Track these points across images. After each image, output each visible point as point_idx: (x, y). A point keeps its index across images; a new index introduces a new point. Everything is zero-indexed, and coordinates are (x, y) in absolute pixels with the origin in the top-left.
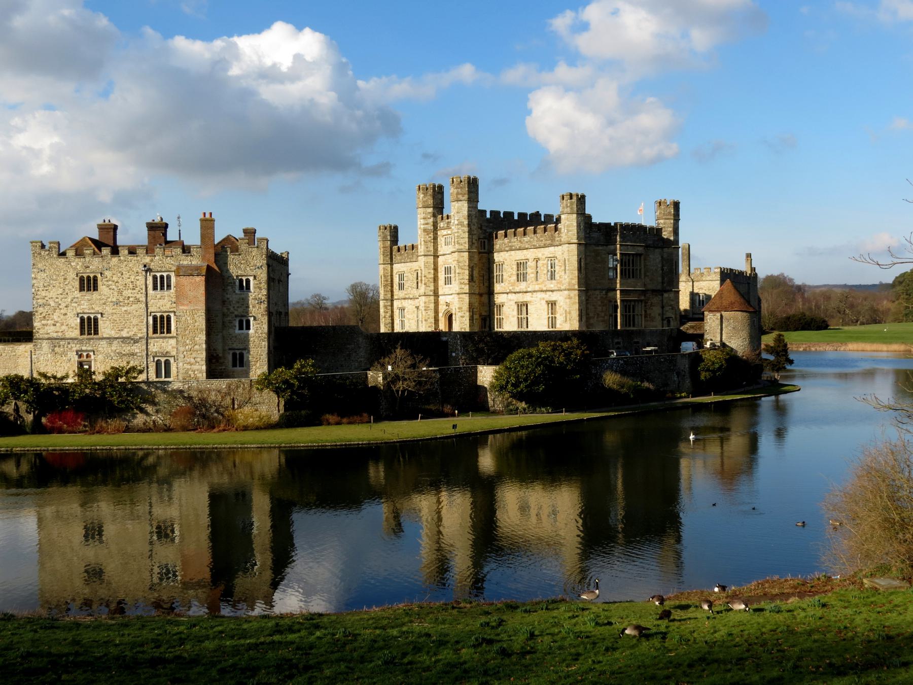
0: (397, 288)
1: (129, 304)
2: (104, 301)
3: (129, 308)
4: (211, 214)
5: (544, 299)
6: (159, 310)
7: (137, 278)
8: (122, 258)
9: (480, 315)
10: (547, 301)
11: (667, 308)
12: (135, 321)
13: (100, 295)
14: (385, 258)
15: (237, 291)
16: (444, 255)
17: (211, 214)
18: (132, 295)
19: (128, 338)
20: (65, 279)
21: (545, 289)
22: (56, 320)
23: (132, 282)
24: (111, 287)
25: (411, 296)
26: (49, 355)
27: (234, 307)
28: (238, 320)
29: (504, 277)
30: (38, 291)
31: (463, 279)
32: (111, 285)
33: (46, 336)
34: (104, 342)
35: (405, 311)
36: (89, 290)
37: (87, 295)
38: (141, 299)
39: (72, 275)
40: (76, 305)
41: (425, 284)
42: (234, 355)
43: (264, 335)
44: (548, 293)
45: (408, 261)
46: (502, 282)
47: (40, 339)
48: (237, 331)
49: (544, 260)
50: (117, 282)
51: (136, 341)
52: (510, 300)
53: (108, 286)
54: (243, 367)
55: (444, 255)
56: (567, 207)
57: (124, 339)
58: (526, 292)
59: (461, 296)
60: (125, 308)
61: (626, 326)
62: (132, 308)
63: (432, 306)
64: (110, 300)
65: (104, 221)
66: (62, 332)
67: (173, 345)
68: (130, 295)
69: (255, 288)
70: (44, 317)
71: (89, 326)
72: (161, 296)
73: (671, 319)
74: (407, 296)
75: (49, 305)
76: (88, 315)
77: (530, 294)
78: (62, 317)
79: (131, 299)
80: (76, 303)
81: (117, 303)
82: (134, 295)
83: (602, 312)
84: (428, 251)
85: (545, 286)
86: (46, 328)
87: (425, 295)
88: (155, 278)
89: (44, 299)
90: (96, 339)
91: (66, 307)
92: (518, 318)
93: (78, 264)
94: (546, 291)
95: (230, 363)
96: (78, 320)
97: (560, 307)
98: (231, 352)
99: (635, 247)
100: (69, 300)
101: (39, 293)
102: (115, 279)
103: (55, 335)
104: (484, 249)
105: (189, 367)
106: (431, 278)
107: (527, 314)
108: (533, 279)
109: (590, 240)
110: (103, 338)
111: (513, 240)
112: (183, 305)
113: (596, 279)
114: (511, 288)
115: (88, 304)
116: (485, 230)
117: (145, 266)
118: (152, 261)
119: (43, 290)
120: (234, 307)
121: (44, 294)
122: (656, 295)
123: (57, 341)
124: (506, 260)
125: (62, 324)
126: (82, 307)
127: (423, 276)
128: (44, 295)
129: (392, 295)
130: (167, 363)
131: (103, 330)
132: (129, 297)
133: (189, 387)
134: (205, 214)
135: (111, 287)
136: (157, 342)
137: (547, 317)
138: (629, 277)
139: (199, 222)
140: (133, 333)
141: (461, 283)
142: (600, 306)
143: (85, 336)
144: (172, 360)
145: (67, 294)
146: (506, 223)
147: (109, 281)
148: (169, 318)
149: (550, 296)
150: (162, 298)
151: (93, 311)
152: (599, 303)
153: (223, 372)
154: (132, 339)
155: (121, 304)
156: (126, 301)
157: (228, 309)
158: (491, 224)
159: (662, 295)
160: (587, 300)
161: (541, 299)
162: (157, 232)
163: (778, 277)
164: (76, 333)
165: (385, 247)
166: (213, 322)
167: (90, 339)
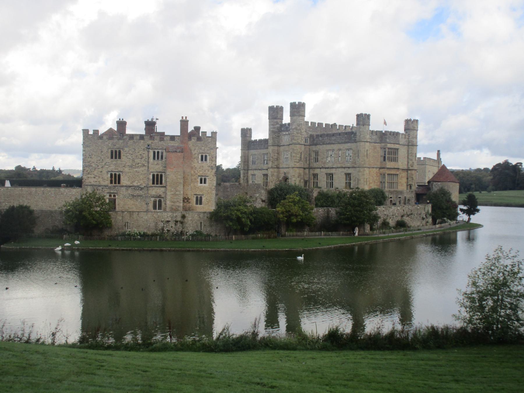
0: (251, 163)
1: (138, 167)
2: (124, 165)
3: (139, 169)
4: (186, 117)
5: (343, 172)
6: (155, 171)
7: (144, 152)
9: (304, 180)
10: (345, 173)
11: (410, 179)
12: (141, 177)
15: (200, 162)
16: (284, 145)
17: (186, 117)
19: (138, 186)
21: (344, 166)
22: (96, 175)
23: (141, 155)
24: (128, 157)
25: (260, 168)
27: (197, 171)
28: (199, 178)
29: (319, 159)
30: (86, 158)
31: (296, 159)
32: (128, 156)
33: (90, 184)
34: (124, 189)
35: (256, 176)
36: (116, 158)
37: (114, 161)
38: (145, 165)
39: (105, 150)
40: (108, 166)
41: (272, 162)
42: (197, 198)
43: (214, 187)
44: (346, 169)
45: (258, 148)
46: (318, 162)
47: (87, 185)
48: (199, 185)
49: (344, 150)
50: (132, 154)
51: (142, 189)
52: (322, 172)
53: (126, 156)
54: (201, 204)
55: (284, 145)
57: (136, 188)
58: (333, 168)
59: (294, 169)
60: (136, 169)
61: (389, 188)
62: (140, 169)
63: (275, 174)
64: (128, 164)
65: (120, 119)
66: (99, 182)
67: (163, 191)
68: (139, 162)
69: (210, 160)
70: (89, 173)
73: (412, 185)
74: (257, 168)
75: (92, 166)
76: (115, 173)
77: (335, 169)
78: (100, 173)
79: (140, 164)
81: (131, 167)
82: (142, 162)
83: (376, 180)
84: (274, 143)
85: (344, 165)
86: (90, 179)
87: (272, 168)
88: (154, 153)
89: (89, 162)
90: (119, 186)
92: (327, 182)
93: (110, 143)
94: (344, 168)
95: (195, 203)
96: (109, 175)
97: (353, 177)
98: (195, 196)
99: (395, 145)
100: (104, 164)
102: (131, 152)
103: (95, 183)
104: (307, 143)
105: (173, 204)
106: (275, 158)
107: (332, 180)
108: (337, 161)
109: (372, 140)
110: (122, 186)
111: (325, 139)
112: (171, 169)
113: (374, 162)
114: (323, 165)
116: (308, 133)
117: (149, 146)
118: (152, 143)
119: (89, 158)
120: (197, 171)
122: (404, 172)
123: (96, 187)
124: (320, 150)
125: (99, 177)
126: (111, 168)
127: (271, 157)
129: (248, 167)
130: (160, 201)
132: (138, 163)
134: (183, 117)
136: (154, 189)
137: (345, 182)
138: (392, 161)
140: (140, 183)
141: (295, 162)
142: (375, 177)
144: (162, 200)
145: (103, 160)
146: (319, 129)
147: (127, 153)
148: (161, 176)
149: (347, 170)
150: (157, 164)
151: (117, 171)
152: (375, 175)
153: (190, 208)
154: (140, 187)
155: (134, 167)
156: (137, 165)
157: (194, 172)
158: (311, 130)
159: (407, 172)
160: (369, 173)
161: (341, 172)
164: (108, 182)
166: (186, 179)
167: (115, 186)
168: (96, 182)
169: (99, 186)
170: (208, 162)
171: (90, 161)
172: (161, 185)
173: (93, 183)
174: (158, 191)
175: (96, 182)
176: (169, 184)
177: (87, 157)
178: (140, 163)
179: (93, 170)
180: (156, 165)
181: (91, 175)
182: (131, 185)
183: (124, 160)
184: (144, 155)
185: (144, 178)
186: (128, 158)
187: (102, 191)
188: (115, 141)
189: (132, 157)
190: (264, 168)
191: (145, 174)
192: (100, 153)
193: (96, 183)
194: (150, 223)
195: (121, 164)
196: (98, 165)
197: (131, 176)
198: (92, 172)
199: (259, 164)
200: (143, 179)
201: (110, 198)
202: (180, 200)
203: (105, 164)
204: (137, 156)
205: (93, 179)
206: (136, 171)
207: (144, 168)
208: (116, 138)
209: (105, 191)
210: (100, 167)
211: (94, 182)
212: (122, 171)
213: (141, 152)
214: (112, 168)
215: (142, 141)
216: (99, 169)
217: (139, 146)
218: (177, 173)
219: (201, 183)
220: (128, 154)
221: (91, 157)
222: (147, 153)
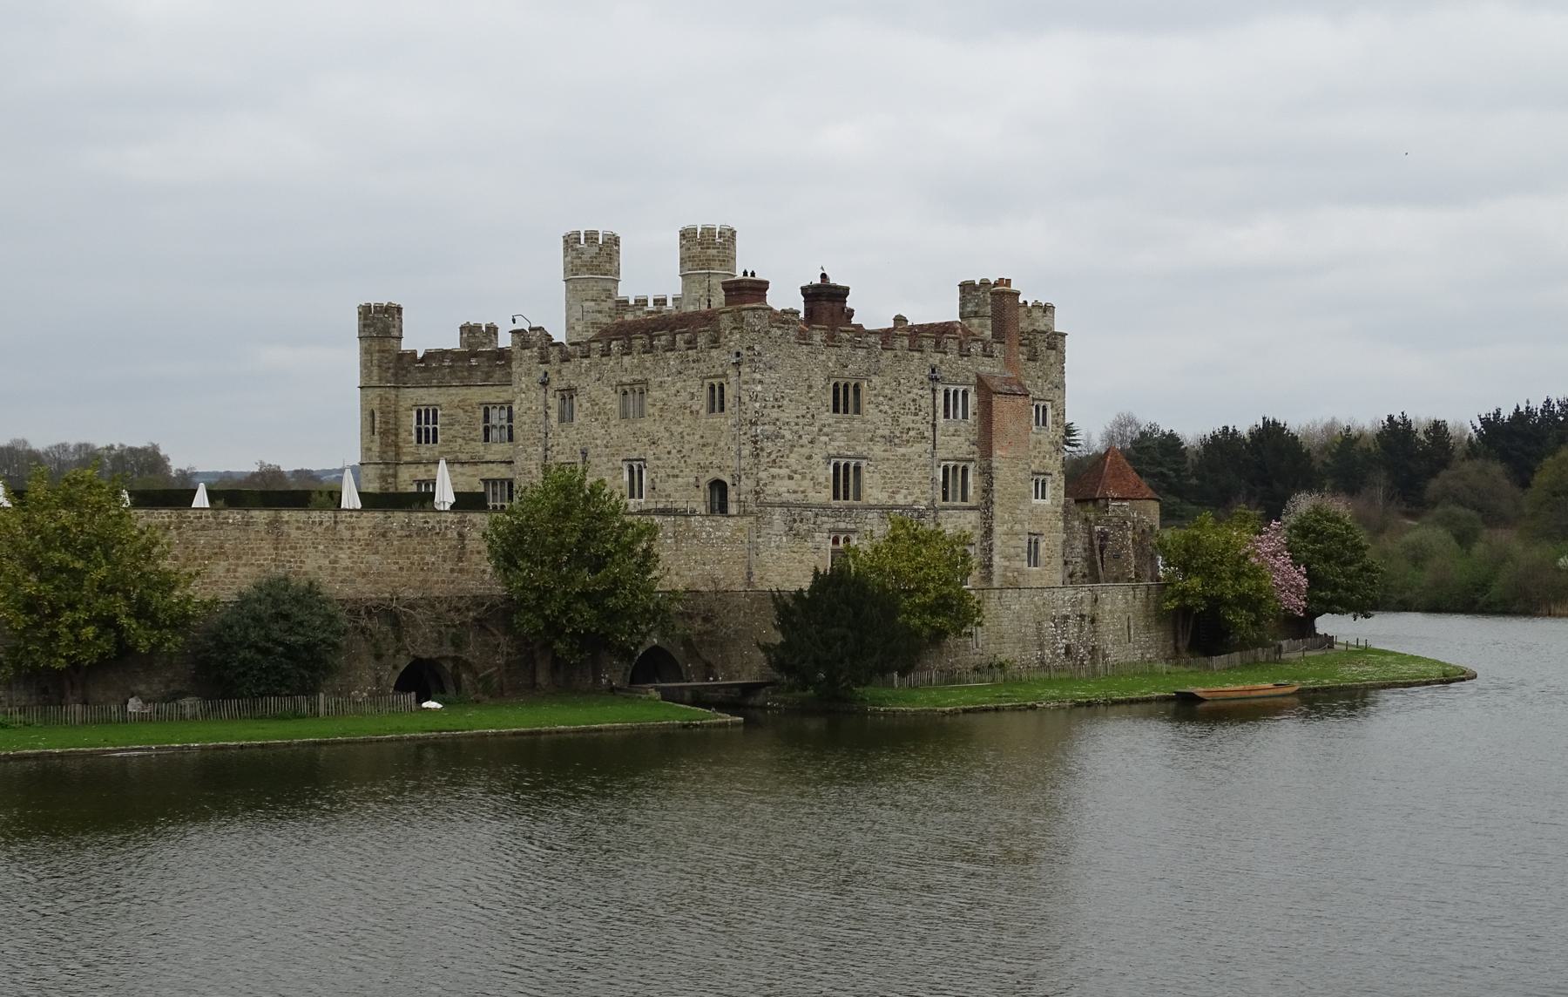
1: (908, 441)
3: (909, 450)
6: (950, 456)
7: (921, 392)
8: (900, 354)
13: (864, 422)
14: (384, 375)
18: (914, 426)
20: (810, 387)
23: (914, 400)
24: (881, 407)
25: (463, 457)
26: (784, 539)
30: (765, 407)
37: (845, 422)
38: (926, 434)
39: (819, 381)
47: (771, 505)
50: (890, 399)
56: (987, 304)
60: (902, 450)
64: (880, 432)
66: (803, 492)
68: (911, 425)
69: (1053, 423)
70: (774, 461)
71: (845, 479)
72: (956, 431)
75: (783, 437)
78: (805, 462)
79: (912, 433)
80: (828, 435)
81: (889, 440)
86: (777, 482)
89: (774, 424)
91: (811, 442)
101: (766, 412)
102: (888, 391)
103: (791, 498)
105: (1007, 564)
115: (840, 438)
117: (933, 371)
119: (773, 407)
121: (775, 414)
123: (798, 510)
125: (804, 478)
128: (774, 415)
131: (869, 491)
132: (909, 429)
133: (1082, 597)
135: (881, 407)
136: (951, 516)
139: (958, 288)
143: (842, 502)
145: (813, 416)
150: (956, 433)
154: (915, 510)
155: (896, 441)
162: (836, 304)
163: (144, 450)
165: (383, 351)
167: (850, 508)
168: (795, 492)
169: (808, 507)
170: (1050, 430)
171: (778, 420)
172: (964, 504)
173: (787, 497)
174: (961, 521)
175: (795, 492)
176: (999, 497)
177: (769, 404)
178: (913, 429)
179: (787, 452)
180: (954, 435)
181: (780, 467)
182: (891, 503)
183: (869, 417)
184: (923, 403)
185: (924, 478)
186: (880, 411)
187: (814, 523)
188: (846, 350)
189: (892, 408)
190: (488, 457)
191: (927, 466)
192: (804, 392)
193: (794, 496)
194: (1026, 626)
195: (864, 431)
196: (801, 433)
197: (889, 471)
198: (782, 457)
199: (460, 441)
200: (920, 483)
201: (836, 547)
202: (1023, 552)
203: (820, 430)
204: (904, 404)
205: (787, 482)
206: (904, 455)
207: (918, 448)
208: (848, 340)
209: (823, 523)
210: (805, 440)
211: (789, 492)
212: (864, 453)
213: (915, 391)
214: (838, 444)
215: (917, 354)
216: (802, 446)
217: (910, 371)
218: (1014, 460)
219: (1037, 497)
220: (881, 398)
221: (779, 407)
222: (931, 396)
